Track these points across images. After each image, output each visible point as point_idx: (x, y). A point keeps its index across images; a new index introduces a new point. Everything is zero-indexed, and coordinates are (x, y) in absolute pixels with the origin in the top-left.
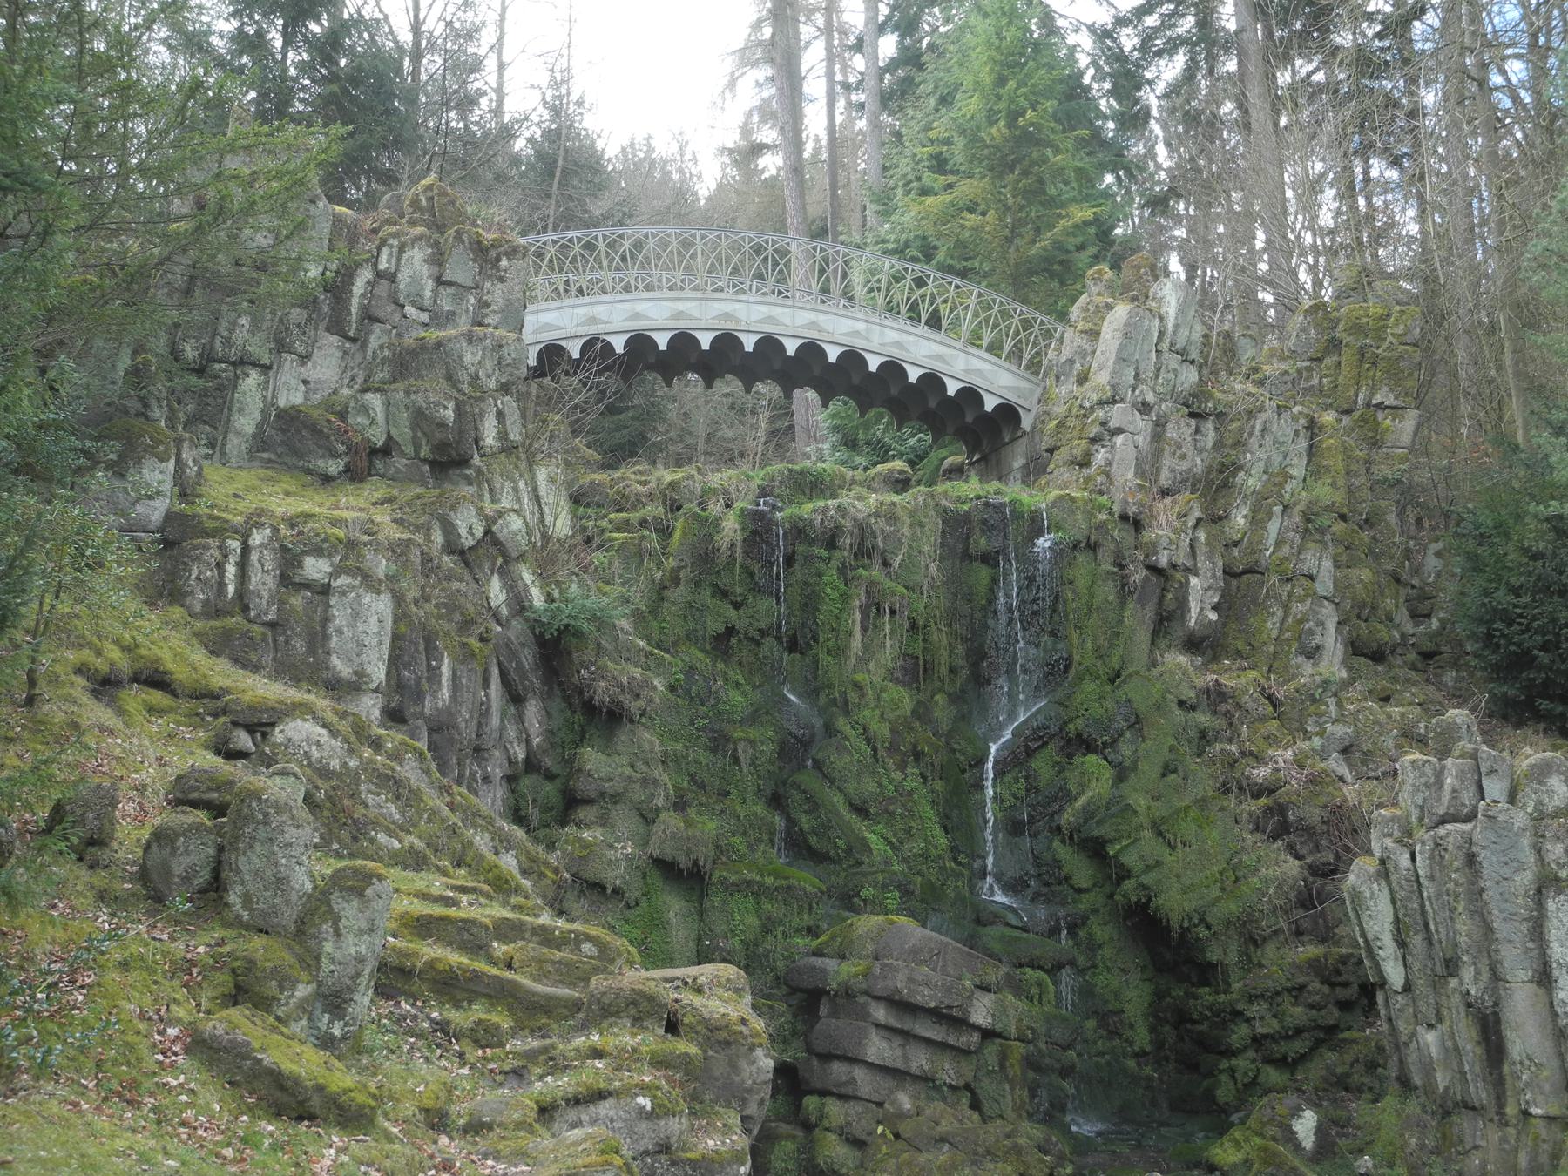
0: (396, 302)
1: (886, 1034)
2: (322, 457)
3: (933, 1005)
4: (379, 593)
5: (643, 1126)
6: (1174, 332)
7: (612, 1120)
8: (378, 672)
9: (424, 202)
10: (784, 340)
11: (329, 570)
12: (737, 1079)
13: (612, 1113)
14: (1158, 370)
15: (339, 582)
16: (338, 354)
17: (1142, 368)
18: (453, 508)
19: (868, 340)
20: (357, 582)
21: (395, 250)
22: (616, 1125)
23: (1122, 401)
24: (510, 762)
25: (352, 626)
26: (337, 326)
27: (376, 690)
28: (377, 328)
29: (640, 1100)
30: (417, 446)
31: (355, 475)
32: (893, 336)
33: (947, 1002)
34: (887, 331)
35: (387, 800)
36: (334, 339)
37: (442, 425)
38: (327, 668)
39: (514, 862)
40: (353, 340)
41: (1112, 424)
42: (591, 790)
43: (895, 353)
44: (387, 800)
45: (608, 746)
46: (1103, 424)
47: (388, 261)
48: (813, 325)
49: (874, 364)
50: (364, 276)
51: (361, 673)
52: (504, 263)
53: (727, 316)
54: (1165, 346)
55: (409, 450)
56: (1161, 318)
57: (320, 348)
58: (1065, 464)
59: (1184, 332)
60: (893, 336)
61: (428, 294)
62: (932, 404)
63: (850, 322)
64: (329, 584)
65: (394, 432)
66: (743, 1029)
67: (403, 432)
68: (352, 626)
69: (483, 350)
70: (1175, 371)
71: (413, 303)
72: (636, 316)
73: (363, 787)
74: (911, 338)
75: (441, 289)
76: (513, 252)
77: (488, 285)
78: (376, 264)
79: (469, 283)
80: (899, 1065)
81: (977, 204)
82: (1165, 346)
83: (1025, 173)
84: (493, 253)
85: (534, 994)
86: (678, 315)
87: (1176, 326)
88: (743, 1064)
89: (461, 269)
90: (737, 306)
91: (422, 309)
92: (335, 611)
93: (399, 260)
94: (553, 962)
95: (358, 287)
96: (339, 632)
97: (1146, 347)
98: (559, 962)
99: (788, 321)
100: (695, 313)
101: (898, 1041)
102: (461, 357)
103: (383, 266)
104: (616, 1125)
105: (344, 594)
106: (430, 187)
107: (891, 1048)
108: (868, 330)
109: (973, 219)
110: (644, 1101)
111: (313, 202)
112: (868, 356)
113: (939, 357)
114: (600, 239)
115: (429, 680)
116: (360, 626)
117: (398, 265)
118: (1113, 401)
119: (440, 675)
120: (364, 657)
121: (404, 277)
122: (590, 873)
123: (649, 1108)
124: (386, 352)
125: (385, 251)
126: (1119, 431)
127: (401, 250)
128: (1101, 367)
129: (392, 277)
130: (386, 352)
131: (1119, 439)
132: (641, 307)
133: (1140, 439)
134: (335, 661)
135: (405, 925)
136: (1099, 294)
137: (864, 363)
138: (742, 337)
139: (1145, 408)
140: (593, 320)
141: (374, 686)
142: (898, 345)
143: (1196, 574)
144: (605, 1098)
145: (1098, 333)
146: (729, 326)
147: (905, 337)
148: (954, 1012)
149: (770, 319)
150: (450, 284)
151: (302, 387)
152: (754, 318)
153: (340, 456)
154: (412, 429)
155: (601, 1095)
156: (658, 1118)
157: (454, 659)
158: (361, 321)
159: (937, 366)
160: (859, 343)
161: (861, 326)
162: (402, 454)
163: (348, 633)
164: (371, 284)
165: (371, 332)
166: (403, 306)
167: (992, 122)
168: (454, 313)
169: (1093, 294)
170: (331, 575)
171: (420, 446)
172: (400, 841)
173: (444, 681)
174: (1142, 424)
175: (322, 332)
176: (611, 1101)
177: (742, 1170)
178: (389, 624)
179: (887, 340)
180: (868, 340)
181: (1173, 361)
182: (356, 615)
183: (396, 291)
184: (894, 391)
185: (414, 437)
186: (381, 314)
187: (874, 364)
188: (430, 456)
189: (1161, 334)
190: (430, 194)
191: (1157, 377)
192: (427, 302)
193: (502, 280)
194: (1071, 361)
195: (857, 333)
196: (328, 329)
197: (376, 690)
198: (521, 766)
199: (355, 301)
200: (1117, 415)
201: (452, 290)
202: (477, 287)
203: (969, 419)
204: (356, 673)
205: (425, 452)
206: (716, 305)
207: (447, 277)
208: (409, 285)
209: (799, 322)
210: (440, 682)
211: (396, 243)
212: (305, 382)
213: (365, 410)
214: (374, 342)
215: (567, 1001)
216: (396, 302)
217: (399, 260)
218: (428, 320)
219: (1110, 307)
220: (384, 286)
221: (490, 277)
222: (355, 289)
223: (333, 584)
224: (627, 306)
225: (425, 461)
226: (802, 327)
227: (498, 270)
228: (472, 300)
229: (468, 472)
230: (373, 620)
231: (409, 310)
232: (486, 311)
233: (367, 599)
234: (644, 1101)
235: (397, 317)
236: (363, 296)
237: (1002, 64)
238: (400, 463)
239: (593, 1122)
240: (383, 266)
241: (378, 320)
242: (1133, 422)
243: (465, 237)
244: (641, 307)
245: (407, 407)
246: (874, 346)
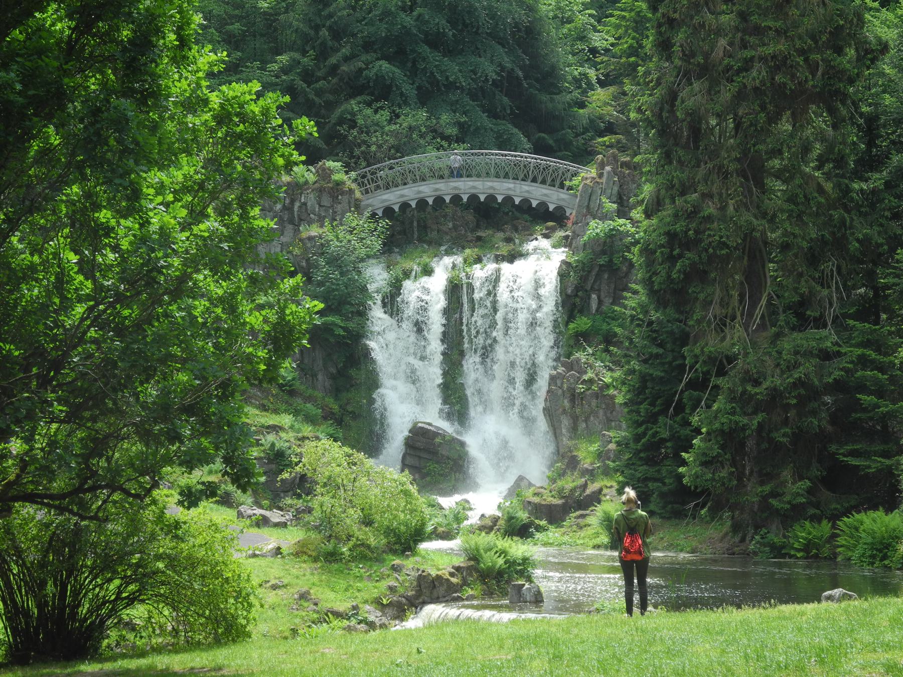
26: (291, 221)
32: (526, 188)
36: (291, 226)
43: (526, 195)
50: (297, 204)
52: (340, 197)
53: (456, 188)
72: (419, 192)
80: (417, 465)
86: (436, 190)
89: (326, 201)
95: (296, 208)
99: (481, 187)
100: (443, 188)
103: (303, 200)
113: (546, 195)
121: (309, 204)
129: (305, 204)
132: (422, 188)
140: (402, 196)
142: (528, 192)
146: (457, 192)
147: (531, 188)
149: (474, 187)
159: (545, 199)
160: (511, 193)
161: (511, 186)
164: (300, 207)
175: (286, 224)
193: (340, 203)
195: (509, 189)
209: (486, 187)
231: (312, 215)
240: (303, 200)
244: (422, 188)
246: (518, 191)
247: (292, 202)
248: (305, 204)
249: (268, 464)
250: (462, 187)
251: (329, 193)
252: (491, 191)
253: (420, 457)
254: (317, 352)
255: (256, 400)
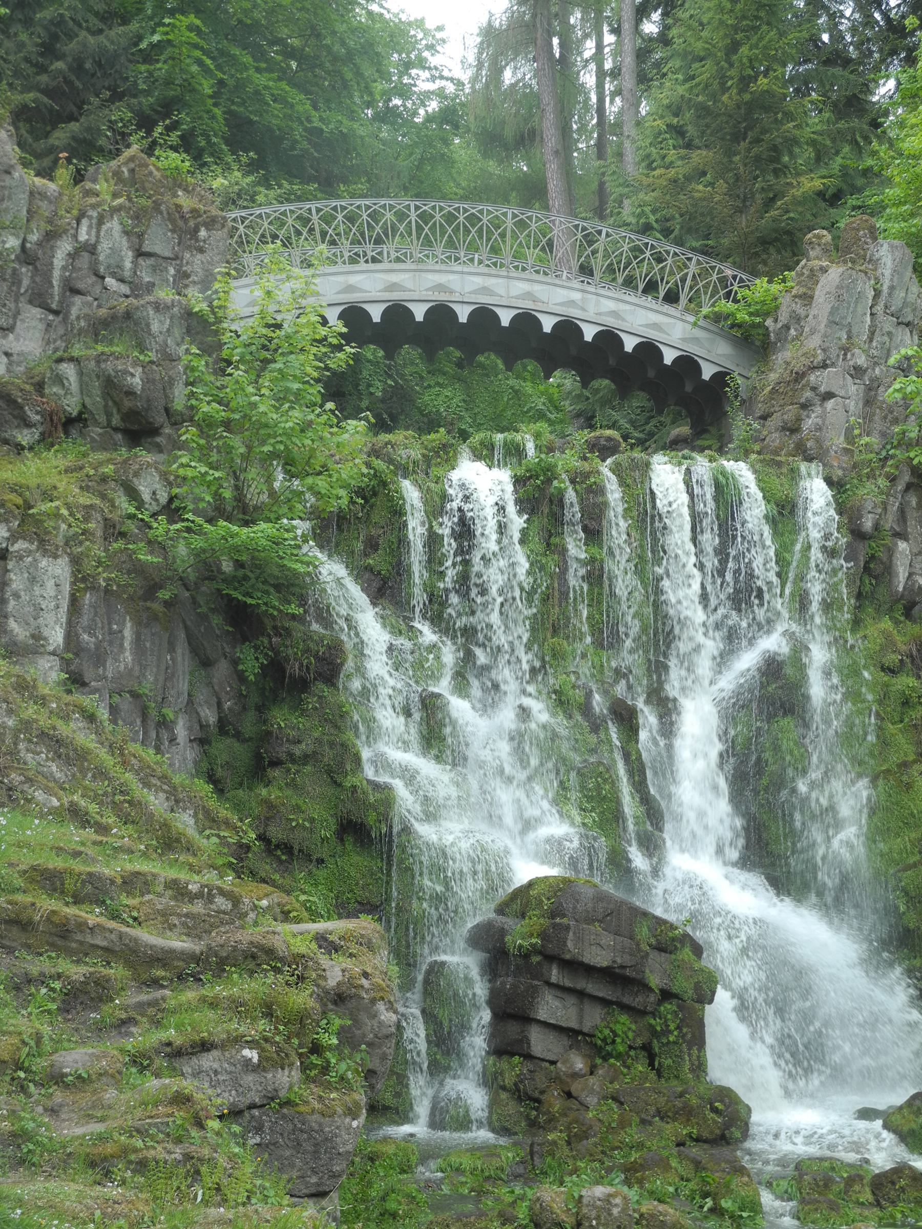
0: (97, 274)
1: (559, 994)
2: (18, 427)
3: (605, 964)
4: (56, 557)
5: (249, 1079)
6: (890, 294)
7: (216, 1072)
8: (56, 637)
9: (126, 174)
10: (498, 311)
11: (7, 535)
12: (358, 1032)
13: (216, 1066)
14: (872, 333)
15: (17, 547)
16: (41, 326)
17: (855, 330)
18: (136, 474)
19: (583, 309)
20: (34, 547)
21: (94, 221)
22: (221, 1078)
23: (833, 365)
24: (201, 726)
25: (29, 590)
26: (39, 299)
27: (53, 653)
28: (78, 300)
29: (247, 1052)
30: (109, 415)
31: (46, 440)
32: (610, 305)
33: (619, 960)
34: (602, 300)
35: (48, 759)
36: (37, 312)
37: (130, 393)
38: (5, 632)
39: (192, 822)
40: (56, 313)
41: (822, 389)
42: (281, 752)
43: (611, 322)
44: (48, 759)
45: (298, 706)
46: (814, 389)
47: (88, 233)
48: (529, 295)
49: (630, 344)
50: (64, 247)
51: (37, 637)
52: (203, 233)
53: (440, 287)
54: (879, 308)
55: (102, 419)
56: (877, 280)
57: (23, 321)
58: (777, 430)
59: (900, 294)
60: (610, 305)
61: (128, 265)
62: (651, 374)
63: (564, 292)
64: (7, 550)
65: (88, 401)
66: (364, 982)
67: (96, 401)
68: (29, 590)
69: (171, 318)
70: (890, 334)
71: (113, 275)
72: (350, 289)
73: (22, 746)
74: (627, 307)
75: (141, 261)
76: (211, 224)
77: (187, 255)
78: (75, 236)
79: (167, 254)
80: (574, 1024)
81: (648, 156)
82: (879, 308)
83: (757, 141)
84: (192, 224)
85: (152, 947)
86: (392, 287)
87: (892, 288)
88: (363, 1017)
90: (452, 277)
91: (122, 281)
92: (12, 576)
93: (98, 232)
94: (179, 915)
95: (59, 259)
96: (17, 596)
97: (860, 310)
98: (187, 915)
99: (502, 292)
100: (409, 285)
101: (571, 1000)
102: (148, 325)
103: (83, 237)
104: (221, 1078)
105: (21, 558)
106: (132, 159)
107: (565, 1007)
108: (583, 299)
109: (700, 189)
110: (252, 1054)
111: (8, 172)
112: (583, 326)
113: (656, 326)
114: (314, 211)
115: (111, 643)
116: (37, 590)
117: (98, 236)
118: (825, 366)
119: (123, 638)
120: (41, 621)
121: (104, 247)
122: (276, 833)
123: (255, 1060)
124: (83, 324)
125: (85, 222)
126: (829, 395)
127: (101, 221)
128: (813, 332)
129: (91, 249)
130: (83, 324)
131: (830, 404)
133: (851, 404)
134: (12, 624)
135: (32, 881)
136: (817, 258)
137: (621, 343)
138: (457, 308)
139: (857, 372)
141: (51, 648)
142: (614, 314)
143: (906, 539)
144: (208, 1050)
145: (812, 297)
146: (443, 297)
148: (628, 972)
149: (485, 290)
150: (149, 255)
151: (5, 360)
152: (467, 289)
153: (34, 425)
154: (104, 398)
155: (205, 1046)
156: (265, 1070)
157: (138, 623)
158: (63, 295)
159: (653, 335)
160: (574, 313)
161: (576, 296)
162: (96, 423)
163: (25, 597)
165: (73, 304)
166: (103, 278)
167: (724, 89)
168: (153, 285)
169: (814, 259)
170: (8, 539)
171: (112, 415)
172: (59, 799)
173: (127, 644)
174: (853, 389)
175: (23, 305)
176: (215, 1053)
177: (355, 1124)
178: (66, 589)
179: (603, 310)
180: (583, 309)
181: (888, 324)
182: (33, 580)
183: (97, 262)
184: (612, 362)
185: (106, 406)
186: (81, 285)
187: (630, 344)
188: (121, 425)
189: (877, 294)
190: (132, 165)
191: (871, 340)
192: (127, 274)
193: (201, 250)
194: (787, 327)
195: (571, 303)
196: (30, 302)
197: (53, 653)
198: (214, 730)
199: (56, 274)
200: (824, 379)
201: (151, 261)
202: (176, 258)
203: (689, 388)
204: (33, 636)
205: (116, 420)
206: (430, 276)
207: (147, 248)
208: (108, 257)
209: (514, 293)
210: (121, 645)
211: (95, 214)
212: (7, 354)
213: (59, 380)
214: (74, 312)
215: (183, 953)
216: (97, 274)
217: (98, 232)
218: (128, 292)
219: (824, 270)
220: (84, 260)
221: (189, 248)
222: (56, 261)
223: (11, 549)
224: (340, 279)
225: (116, 429)
226: (517, 297)
227: (197, 240)
228: (172, 271)
229: (158, 439)
230: (50, 584)
231: (108, 280)
232: (186, 282)
233: (44, 563)
234: (252, 1054)
235: (98, 289)
236: (64, 268)
237: (736, 28)
238: (95, 431)
239: (196, 1074)
240: (83, 237)
241: (78, 292)
242: (844, 386)
243: (163, 208)
244: (354, 280)
245: (98, 377)
247: (51, 236)
248: (91, 249)
249: (258, 1068)
250: (456, 287)
251: (173, 221)
252: (528, 305)
253: (581, 994)
254: (179, 651)
255: (48, 791)
